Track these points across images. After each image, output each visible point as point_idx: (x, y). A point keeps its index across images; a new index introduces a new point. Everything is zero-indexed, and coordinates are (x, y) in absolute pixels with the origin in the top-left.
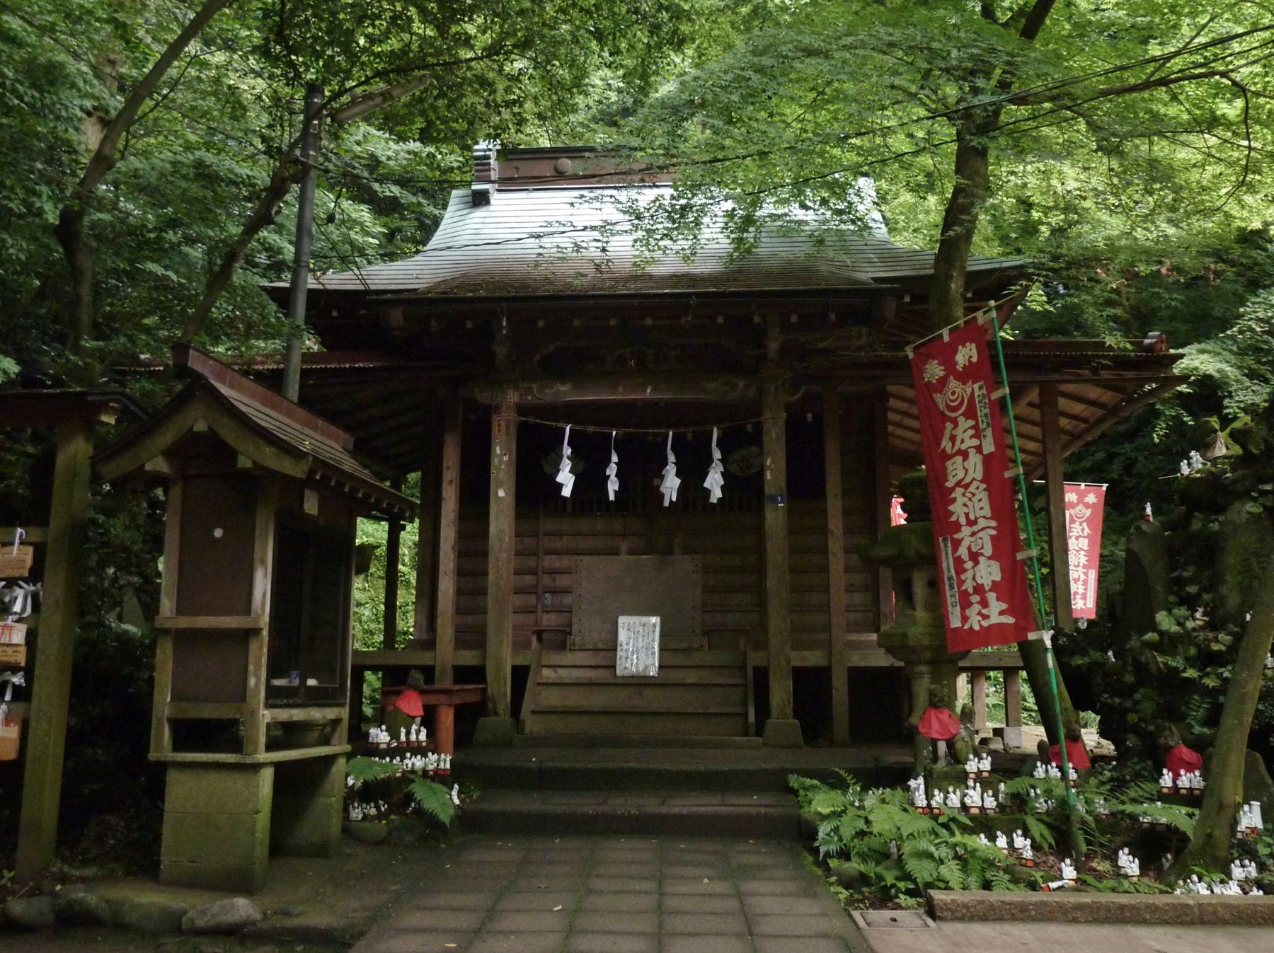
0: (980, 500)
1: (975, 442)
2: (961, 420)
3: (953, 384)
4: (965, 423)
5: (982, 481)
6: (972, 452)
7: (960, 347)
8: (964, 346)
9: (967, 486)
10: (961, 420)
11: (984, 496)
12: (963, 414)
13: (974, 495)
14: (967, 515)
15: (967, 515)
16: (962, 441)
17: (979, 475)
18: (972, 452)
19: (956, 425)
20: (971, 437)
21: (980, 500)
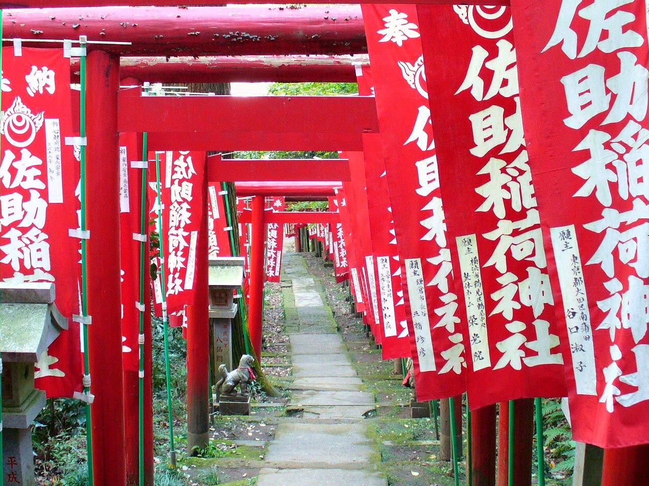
0: (39, 250)
1: (40, 185)
2: (26, 153)
3: (19, 106)
4: (29, 159)
5: (43, 230)
6: (35, 195)
7: (34, 68)
8: (40, 69)
9: (25, 230)
10: (26, 153)
11: (46, 247)
12: (27, 148)
13: (32, 242)
14: (21, 261)
15: (21, 261)
16: (24, 179)
17: (41, 222)
18: (35, 195)
19: (18, 157)
20: (36, 177)
21: (39, 250)
